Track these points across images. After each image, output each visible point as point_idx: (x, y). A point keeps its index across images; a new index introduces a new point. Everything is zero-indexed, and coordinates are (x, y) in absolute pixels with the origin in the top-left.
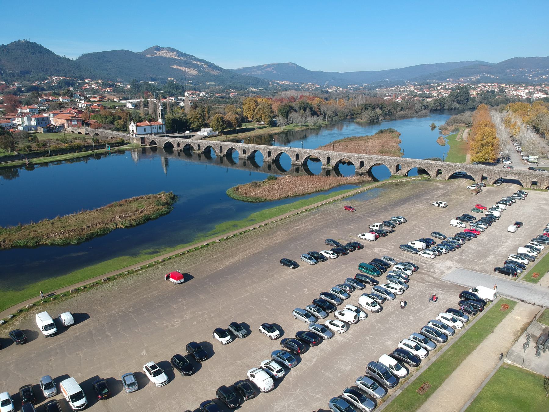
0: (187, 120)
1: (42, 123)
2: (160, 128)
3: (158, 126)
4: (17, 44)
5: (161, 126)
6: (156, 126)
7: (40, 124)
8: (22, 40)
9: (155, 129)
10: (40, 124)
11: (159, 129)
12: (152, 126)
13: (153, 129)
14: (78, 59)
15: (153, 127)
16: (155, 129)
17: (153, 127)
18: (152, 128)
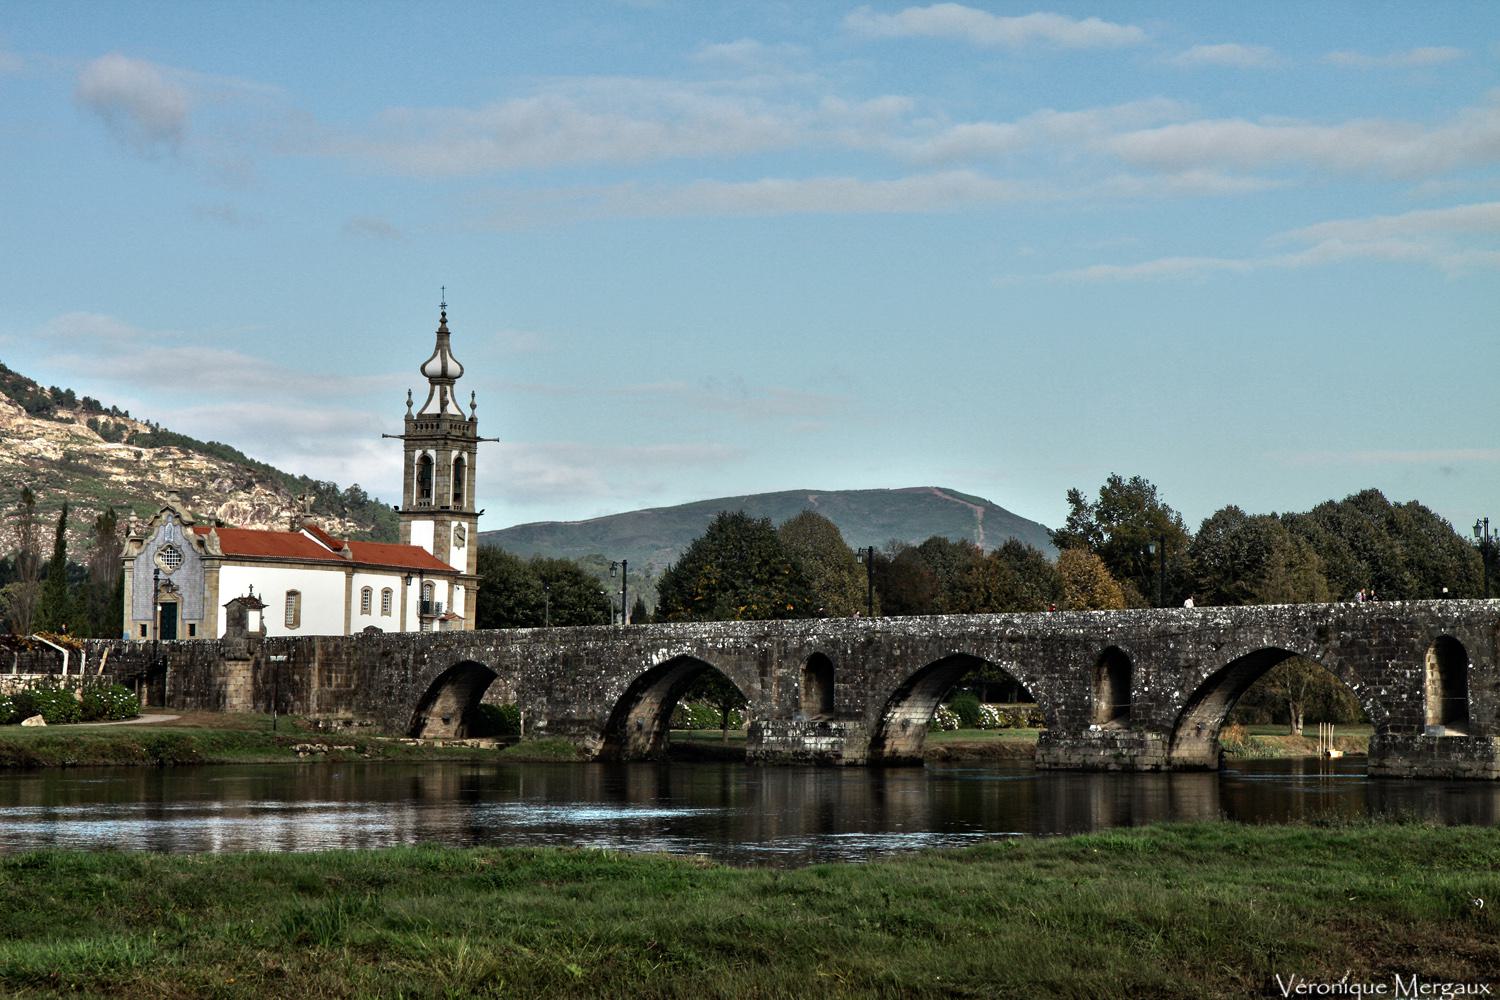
6: (394, 581)
15: (367, 592)
17: (367, 592)
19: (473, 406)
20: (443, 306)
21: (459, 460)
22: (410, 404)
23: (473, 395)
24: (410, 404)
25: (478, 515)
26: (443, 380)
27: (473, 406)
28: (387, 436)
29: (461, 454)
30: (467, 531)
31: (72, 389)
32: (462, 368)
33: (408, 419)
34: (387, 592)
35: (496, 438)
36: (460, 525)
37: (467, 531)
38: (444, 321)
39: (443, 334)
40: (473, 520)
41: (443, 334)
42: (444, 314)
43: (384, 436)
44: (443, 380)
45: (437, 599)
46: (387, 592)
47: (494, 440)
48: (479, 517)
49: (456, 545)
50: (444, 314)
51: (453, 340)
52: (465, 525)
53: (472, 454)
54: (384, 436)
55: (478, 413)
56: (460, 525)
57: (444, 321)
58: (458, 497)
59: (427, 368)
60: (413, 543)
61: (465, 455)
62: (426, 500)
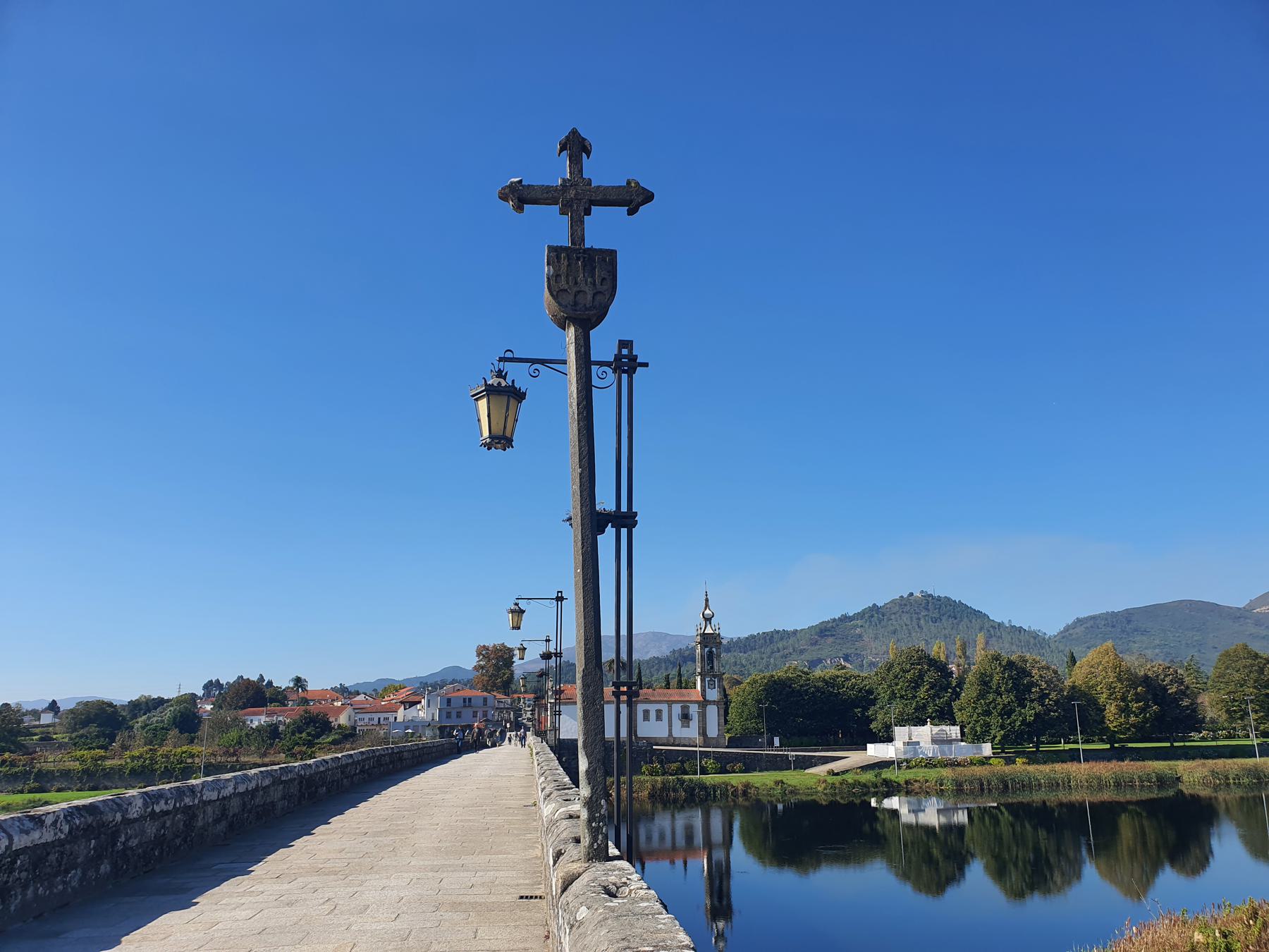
0: (870, 692)
1: (459, 715)
2: (686, 717)
3: (677, 709)
4: (905, 604)
5: (694, 710)
6: (664, 707)
7: (454, 715)
8: (917, 594)
9: (659, 718)
10: (454, 715)
11: (677, 723)
12: (640, 708)
13: (646, 717)
14: (1062, 632)
15: (646, 713)
16: (659, 718)
17: (646, 713)
18: (640, 716)
21: (711, 652)
26: (708, 620)
31: (490, 643)
34: (659, 712)
38: (706, 595)
39: (707, 600)
41: (707, 600)
44: (708, 620)
46: (659, 712)
49: (709, 688)
51: (710, 603)
57: (706, 595)
61: (714, 649)
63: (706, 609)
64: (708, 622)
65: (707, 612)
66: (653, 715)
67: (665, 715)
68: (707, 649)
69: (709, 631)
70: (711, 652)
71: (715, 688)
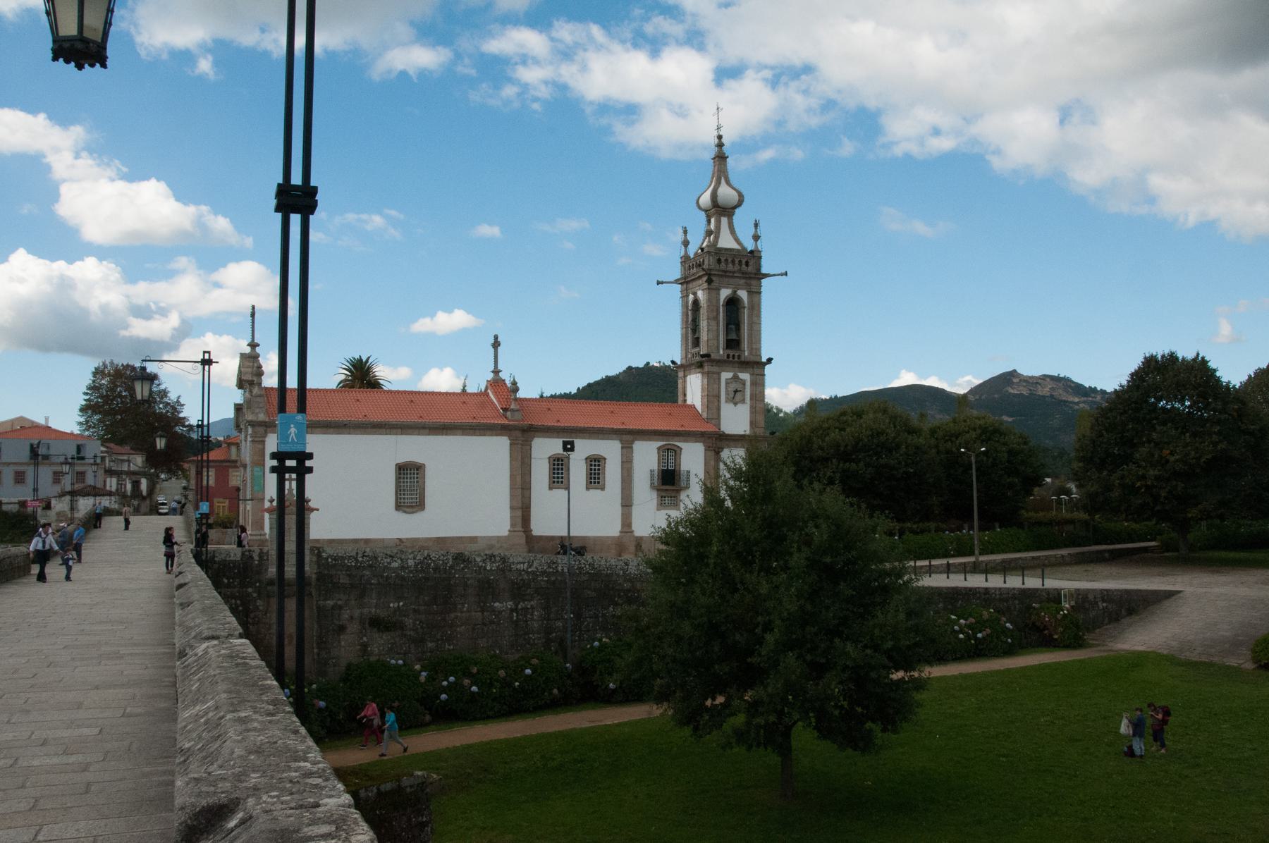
3: (647, 456)
6: (610, 450)
19: (756, 238)
20: (719, 128)
21: (733, 302)
22: (686, 243)
23: (756, 225)
24: (686, 243)
25: (765, 364)
26: (720, 210)
27: (756, 238)
28: (662, 283)
29: (735, 292)
30: (748, 384)
32: (741, 195)
33: (685, 259)
35: (784, 271)
36: (736, 378)
37: (748, 384)
40: (757, 371)
42: (720, 137)
43: (659, 283)
44: (720, 210)
45: (684, 466)
47: (782, 275)
48: (767, 368)
50: (720, 137)
52: (745, 376)
53: (755, 293)
54: (659, 283)
55: (763, 246)
56: (736, 378)
58: (733, 344)
59: (701, 201)
60: (689, 402)
61: (743, 294)
62: (697, 349)
63: (718, 183)
64: (724, 220)
65: (726, 193)
66: (578, 471)
67: (613, 472)
68: (725, 293)
69: (726, 242)
70: (733, 302)
71: (743, 401)
